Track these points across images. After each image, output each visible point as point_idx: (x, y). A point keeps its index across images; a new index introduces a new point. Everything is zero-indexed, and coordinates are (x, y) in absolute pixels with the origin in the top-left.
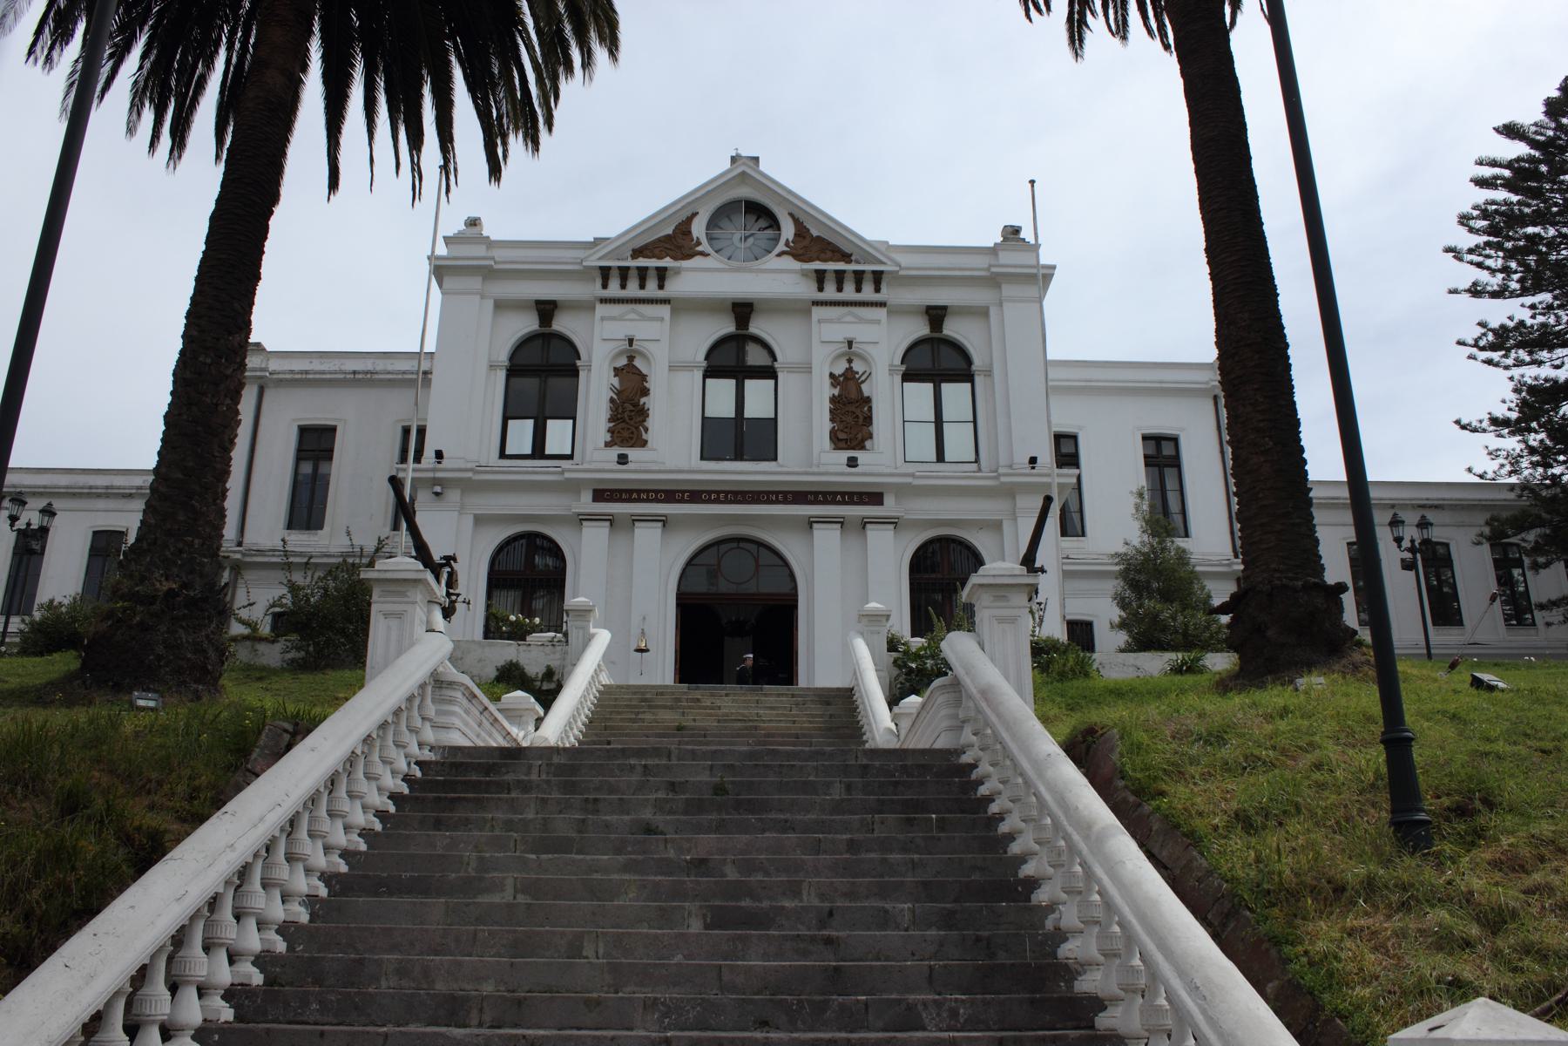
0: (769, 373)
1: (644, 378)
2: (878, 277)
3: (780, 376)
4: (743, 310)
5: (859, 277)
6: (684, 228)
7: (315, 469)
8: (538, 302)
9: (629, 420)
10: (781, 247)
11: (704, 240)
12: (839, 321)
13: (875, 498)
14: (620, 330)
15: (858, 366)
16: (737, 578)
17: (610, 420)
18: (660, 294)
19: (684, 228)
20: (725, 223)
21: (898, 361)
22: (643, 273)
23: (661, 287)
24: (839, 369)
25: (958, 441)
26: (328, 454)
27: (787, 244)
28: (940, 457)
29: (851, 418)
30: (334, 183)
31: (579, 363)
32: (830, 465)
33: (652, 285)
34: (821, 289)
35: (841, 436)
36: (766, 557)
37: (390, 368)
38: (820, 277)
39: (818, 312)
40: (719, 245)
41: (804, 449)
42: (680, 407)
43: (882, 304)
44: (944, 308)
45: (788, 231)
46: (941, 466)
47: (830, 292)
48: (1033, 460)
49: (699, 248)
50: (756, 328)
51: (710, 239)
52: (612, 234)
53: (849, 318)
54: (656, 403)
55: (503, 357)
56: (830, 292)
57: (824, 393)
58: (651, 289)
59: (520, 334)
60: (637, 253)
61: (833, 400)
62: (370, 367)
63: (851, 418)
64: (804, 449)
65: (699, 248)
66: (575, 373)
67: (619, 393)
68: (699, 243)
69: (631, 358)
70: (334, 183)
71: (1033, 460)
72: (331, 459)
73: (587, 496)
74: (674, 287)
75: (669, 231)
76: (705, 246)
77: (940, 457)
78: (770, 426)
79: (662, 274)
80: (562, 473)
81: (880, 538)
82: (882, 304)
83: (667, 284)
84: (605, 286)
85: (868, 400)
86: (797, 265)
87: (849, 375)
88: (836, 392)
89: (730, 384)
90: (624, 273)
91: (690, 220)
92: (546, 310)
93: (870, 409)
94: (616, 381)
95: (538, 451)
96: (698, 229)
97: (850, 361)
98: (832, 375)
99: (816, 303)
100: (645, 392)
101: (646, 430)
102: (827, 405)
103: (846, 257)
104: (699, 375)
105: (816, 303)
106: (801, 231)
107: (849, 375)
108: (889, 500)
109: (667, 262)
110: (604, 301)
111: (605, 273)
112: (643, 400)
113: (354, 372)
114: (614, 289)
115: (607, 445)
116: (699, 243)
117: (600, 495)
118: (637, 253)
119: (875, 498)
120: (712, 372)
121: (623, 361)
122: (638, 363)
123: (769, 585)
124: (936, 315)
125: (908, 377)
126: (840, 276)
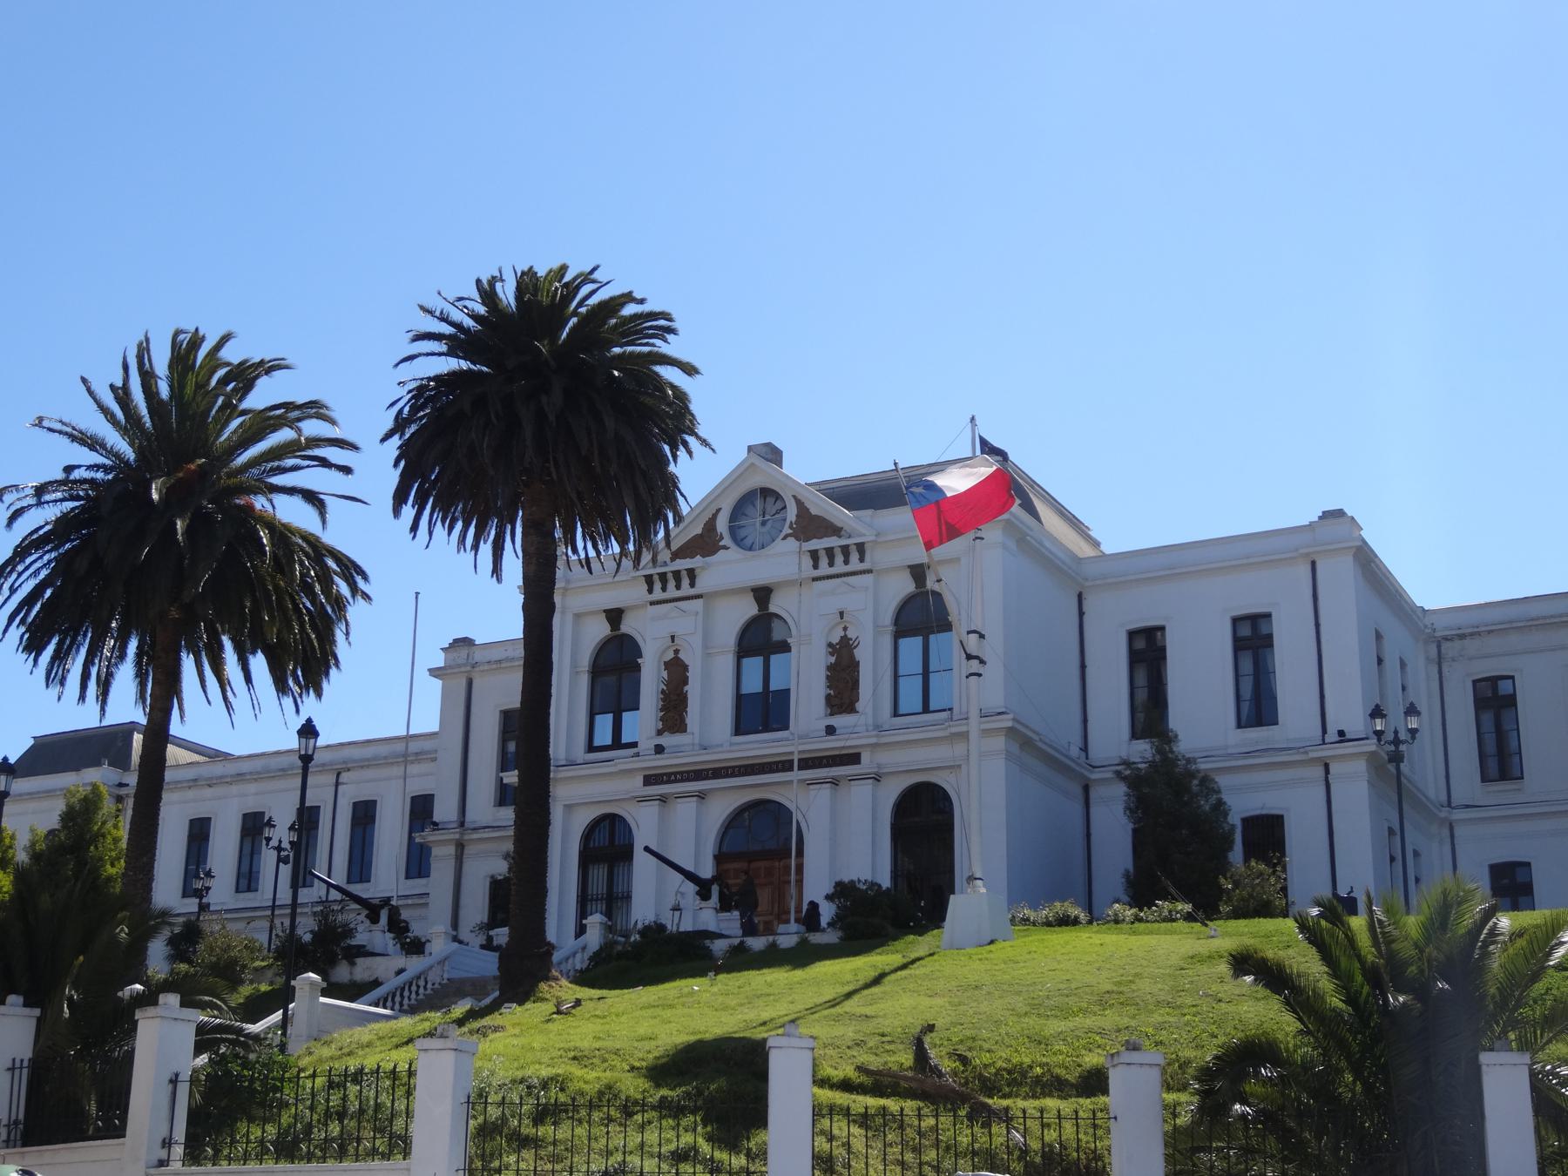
1: (685, 668)
2: (861, 548)
4: (762, 594)
5: (845, 550)
6: (710, 525)
10: (787, 530)
13: (854, 759)
15: (851, 634)
18: (692, 592)
19: (710, 525)
20: (749, 510)
22: (677, 574)
24: (835, 640)
28: (926, 709)
29: (843, 688)
38: (814, 555)
43: (869, 571)
45: (792, 513)
47: (824, 569)
51: (733, 531)
54: (693, 690)
58: (686, 589)
61: (830, 668)
63: (843, 688)
73: (640, 780)
74: (703, 584)
75: (698, 530)
79: (692, 574)
81: (861, 793)
82: (869, 571)
83: (698, 582)
84: (650, 591)
88: (833, 660)
89: (759, 660)
91: (715, 516)
92: (614, 616)
94: (665, 674)
95: (617, 744)
96: (722, 525)
97: (845, 629)
98: (830, 645)
99: (815, 579)
100: (685, 681)
105: (815, 579)
108: (865, 758)
109: (696, 562)
110: (652, 603)
114: (658, 594)
116: (722, 538)
117: (649, 780)
119: (854, 759)
121: (670, 655)
126: (830, 552)
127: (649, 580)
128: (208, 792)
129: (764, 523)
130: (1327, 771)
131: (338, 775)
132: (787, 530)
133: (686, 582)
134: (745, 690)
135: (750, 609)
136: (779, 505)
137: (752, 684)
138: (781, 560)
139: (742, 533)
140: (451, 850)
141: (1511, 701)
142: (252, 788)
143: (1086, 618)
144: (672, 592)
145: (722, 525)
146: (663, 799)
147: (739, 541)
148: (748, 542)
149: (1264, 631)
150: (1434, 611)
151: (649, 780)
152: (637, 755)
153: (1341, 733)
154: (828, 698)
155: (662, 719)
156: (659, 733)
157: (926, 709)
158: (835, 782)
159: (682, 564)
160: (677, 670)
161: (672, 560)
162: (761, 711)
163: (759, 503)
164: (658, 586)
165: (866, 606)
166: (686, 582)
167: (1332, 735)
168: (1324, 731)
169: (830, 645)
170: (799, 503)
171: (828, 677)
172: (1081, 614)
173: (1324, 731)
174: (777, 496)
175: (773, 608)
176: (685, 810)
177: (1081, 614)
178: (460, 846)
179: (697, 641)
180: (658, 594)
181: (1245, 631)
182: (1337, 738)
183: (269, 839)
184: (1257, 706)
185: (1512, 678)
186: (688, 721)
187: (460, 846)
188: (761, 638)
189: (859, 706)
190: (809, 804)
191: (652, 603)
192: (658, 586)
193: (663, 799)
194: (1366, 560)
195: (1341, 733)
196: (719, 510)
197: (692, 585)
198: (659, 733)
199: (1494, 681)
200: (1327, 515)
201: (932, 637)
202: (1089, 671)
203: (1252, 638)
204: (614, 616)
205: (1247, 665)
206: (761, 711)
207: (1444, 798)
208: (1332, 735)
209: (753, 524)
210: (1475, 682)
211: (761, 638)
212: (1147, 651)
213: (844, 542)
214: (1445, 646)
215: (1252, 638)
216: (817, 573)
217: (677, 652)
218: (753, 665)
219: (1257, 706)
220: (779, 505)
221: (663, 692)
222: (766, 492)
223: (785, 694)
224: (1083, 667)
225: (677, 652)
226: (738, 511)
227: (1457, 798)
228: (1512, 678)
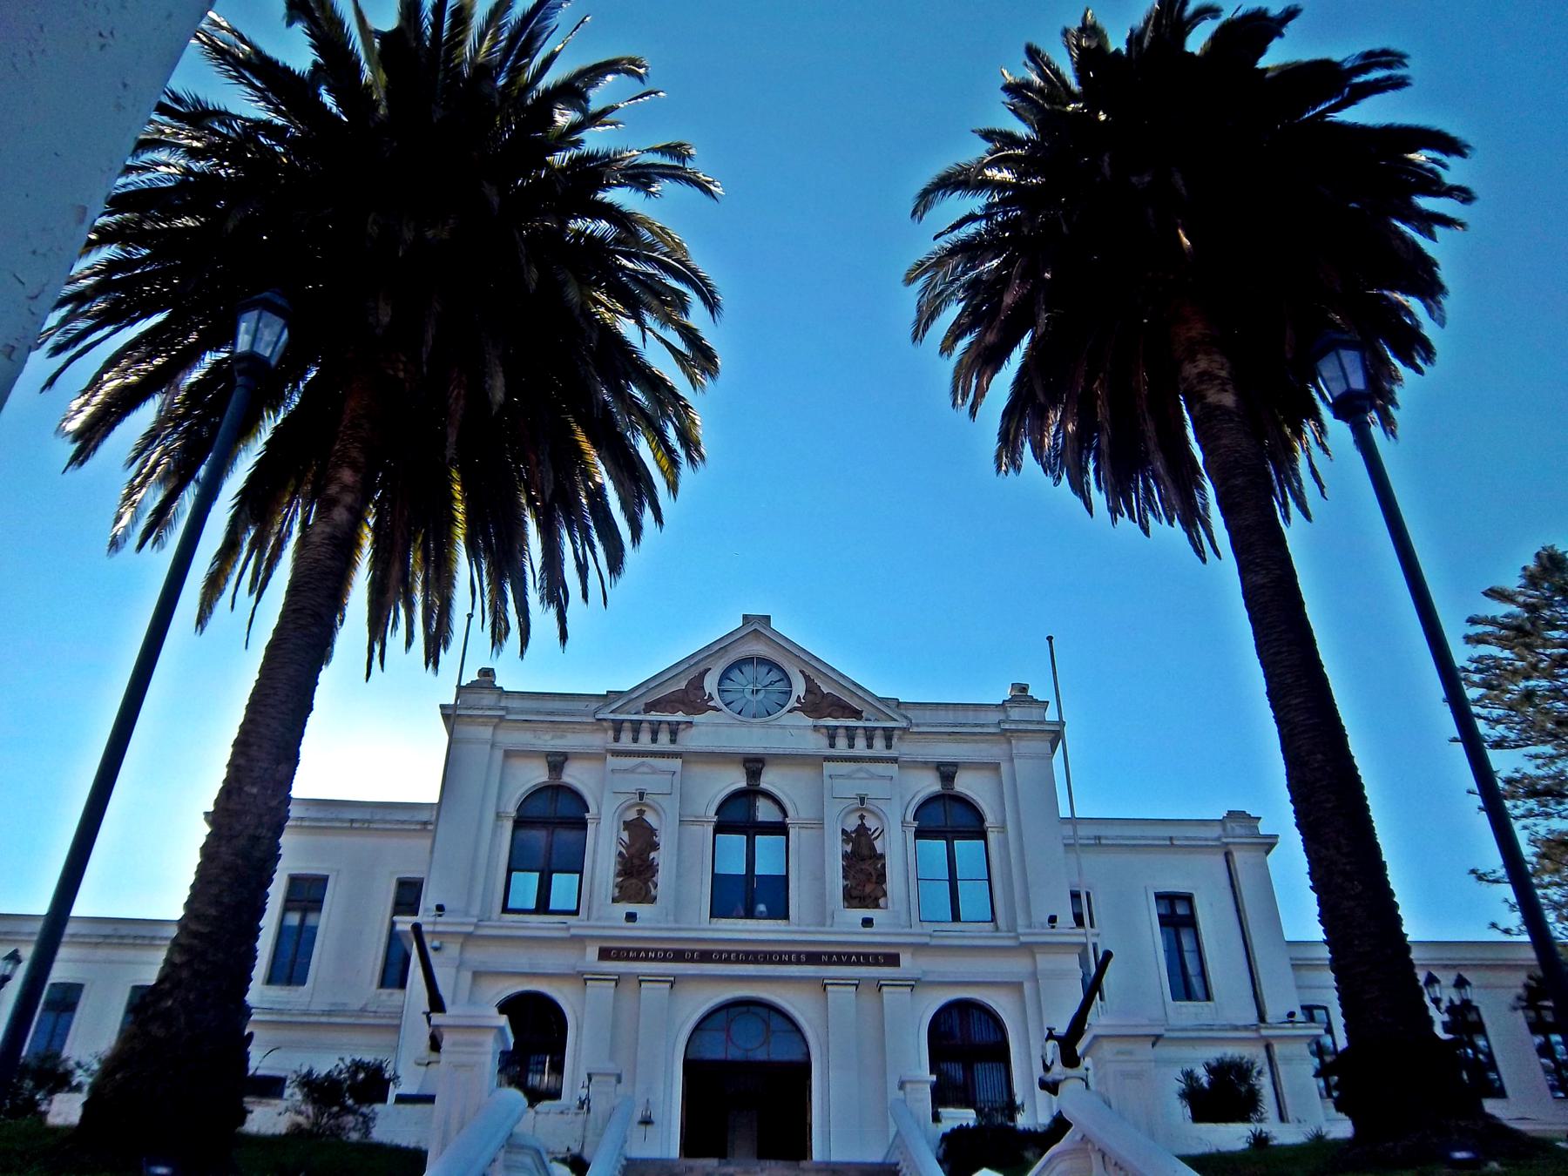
0: (780, 829)
3: (792, 832)
4: (754, 765)
6: (697, 683)
7: (303, 920)
8: (548, 754)
9: (636, 874)
10: (792, 703)
11: (716, 695)
12: (849, 777)
14: (850, 789)
15: (871, 823)
16: (749, 1045)
17: (618, 875)
18: (673, 748)
21: (910, 817)
23: (673, 741)
24: (852, 823)
25: (972, 897)
26: (316, 904)
28: (956, 917)
29: (864, 876)
30: (564, 636)
31: (587, 816)
32: (847, 925)
33: (664, 738)
34: (832, 746)
35: (855, 893)
36: (776, 1021)
37: (388, 817)
38: (832, 735)
39: (829, 767)
40: (729, 697)
41: (818, 910)
42: (691, 860)
43: (895, 760)
44: (955, 765)
45: (799, 688)
46: (958, 926)
48: (1053, 919)
50: (768, 781)
53: (862, 775)
54: (663, 858)
55: (511, 810)
57: (836, 851)
59: (968, 792)
60: (649, 707)
61: (845, 856)
62: (368, 817)
63: (864, 876)
64: (818, 910)
66: (582, 825)
67: (628, 847)
68: (711, 698)
69: (641, 812)
70: (564, 636)
71: (1053, 919)
72: (320, 910)
73: (592, 952)
76: (717, 701)
77: (956, 917)
78: (781, 883)
80: (568, 928)
82: (895, 760)
84: (617, 739)
85: (882, 856)
86: (810, 721)
87: (862, 829)
89: (740, 840)
90: (636, 727)
93: (884, 866)
94: (625, 836)
95: (543, 906)
96: (710, 684)
98: (844, 831)
99: (828, 759)
100: (655, 847)
101: (656, 886)
102: (840, 863)
103: (857, 714)
104: (711, 829)
105: (828, 759)
106: (811, 688)
107: (862, 829)
108: (905, 959)
109: (679, 716)
110: (616, 753)
111: (618, 727)
112: (652, 855)
113: (352, 821)
114: (626, 742)
115: (614, 900)
119: (893, 960)
120: (720, 828)
123: (781, 1052)
124: (946, 772)
125: (920, 834)
134: (719, 870)
137: (735, 865)
151: (605, 954)
170: (807, 678)
179: (671, 807)
180: (626, 742)
218: (735, 843)
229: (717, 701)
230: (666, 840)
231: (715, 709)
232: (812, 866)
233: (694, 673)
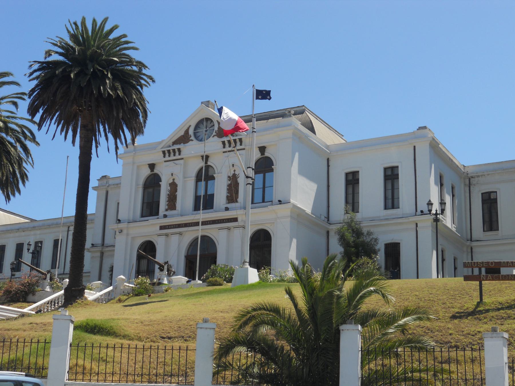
15: (237, 173)
18: (179, 157)
20: (201, 126)
22: (174, 150)
24: (231, 175)
27: (216, 132)
38: (224, 143)
45: (216, 128)
49: (191, 139)
51: (195, 134)
52: (165, 138)
54: (179, 194)
56: (227, 149)
65: (191, 139)
73: (158, 228)
76: (193, 138)
83: (182, 153)
88: (230, 182)
90: (169, 151)
92: (152, 166)
94: (169, 188)
96: (191, 132)
98: (229, 177)
100: (176, 191)
109: (181, 146)
110: (165, 161)
116: (191, 136)
117: (162, 228)
118: (174, 143)
121: (171, 181)
122: (175, 181)
127: (164, 152)
128: (23, 234)
129: (206, 131)
130: (417, 226)
131: (69, 227)
132: (214, 134)
133: (177, 153)
135: (201, 164)
136: (212, 124)
138: (213, 145)
139: (198, 134)
140: (99, 254)
141: (495, 201)
142: (38, 232)
143: (330, 168)
144: (172, 157)
145: (191, 132)
146: (167, 235)
147: (197, 138)
148: (200, 138)
149: (396, 173)
150: (468, 167)
152: (158, 218)
153: (422, 212)
154: (227, 197)
155: (168, 205)
156: (167, 210)
157: (263, 201)
158: (229, 229)
159: (176, 147)
160: (173, 186)
161: (173, 145)
162: (204, 202)
163: (205, 123)
164: (167, 155)
165: (243, 161)
166: (177, 153)
167: (419, 212)
168: (416, 211)
169: (229, 177)
171: (228, 189)
172: (328, 166)
173: (416, 211)
174: (212, 121)
175: (209, 163)
176: (175, 239)
177: (328, 166)
178: (102, 253)
179: (181, 176)
180: (167, 158)
181: (389, 172)
182: (421, 214)
183: (28, 250)
184: (391, 201)
185: (496, 192)
186: (177, 205)
187: (102, 253)
188: (205, 175)
189: (239, 200)
190: (219, 235)
191: (165, 161)
192: (167, 155)
193: (167, 235)
194: (435, 147)
195: (422, 212)
196: (190, 126)
197: (180, 154)
198: (167, 210)
199: (489, 193)
200: (420, 128)
201: (267, 174)
202: (330, 188)
203: (391, 175)
204: (152, 166)
205: (389, 186)
206: (204, 202)
207: (469, 237)
208: (419, 212)
209: (202, 130)
210: (482, 194)
211: (205, 175)
212: (352, 180)
213: (234, 138)
214: (472, 180)
215: (391, 175)
216: (225, 150)
217: (174, 179)
219: (391, 201)
220: (212, 124)
221: (168, 195)
222: (208, 119)
223: (212, 196)
224: (328, 186)
225: (174, 179)
226: (197, 126)
227: (474, 237)
228: (496, 192)
229: (193, 138)
230: (179, 188)
231: (192, 140)
232: (220, 190)
233: (185, 128)
